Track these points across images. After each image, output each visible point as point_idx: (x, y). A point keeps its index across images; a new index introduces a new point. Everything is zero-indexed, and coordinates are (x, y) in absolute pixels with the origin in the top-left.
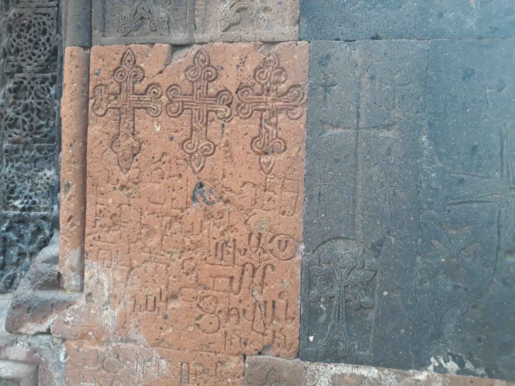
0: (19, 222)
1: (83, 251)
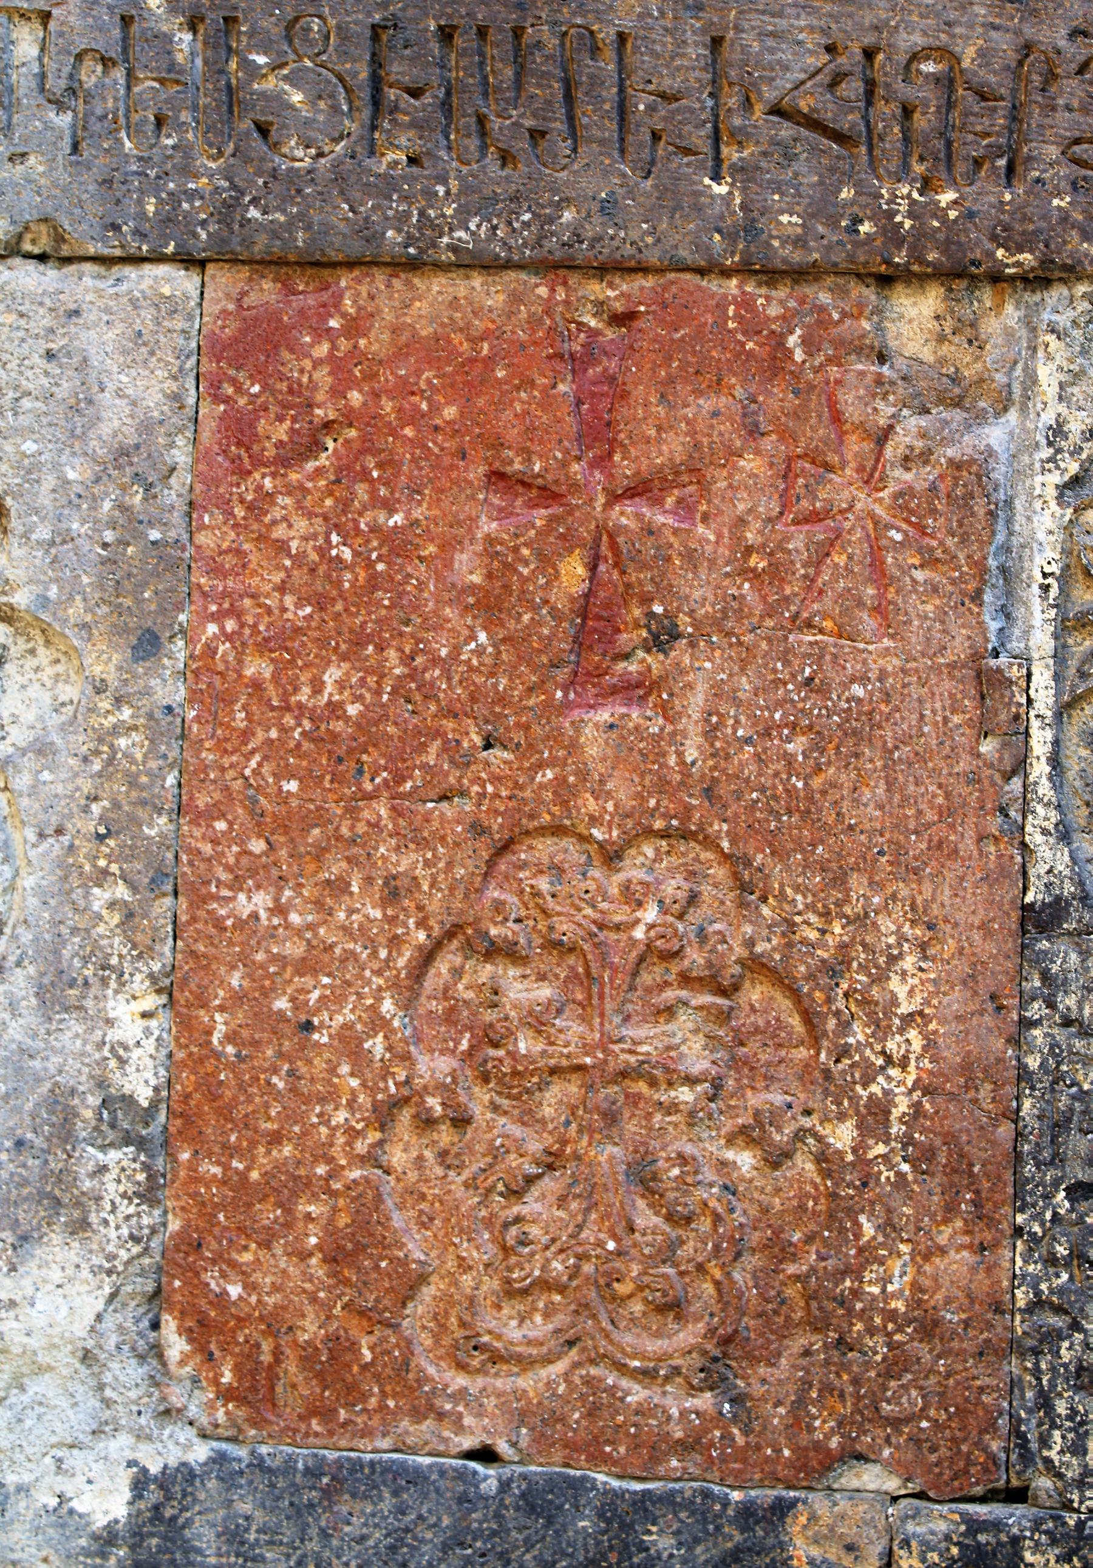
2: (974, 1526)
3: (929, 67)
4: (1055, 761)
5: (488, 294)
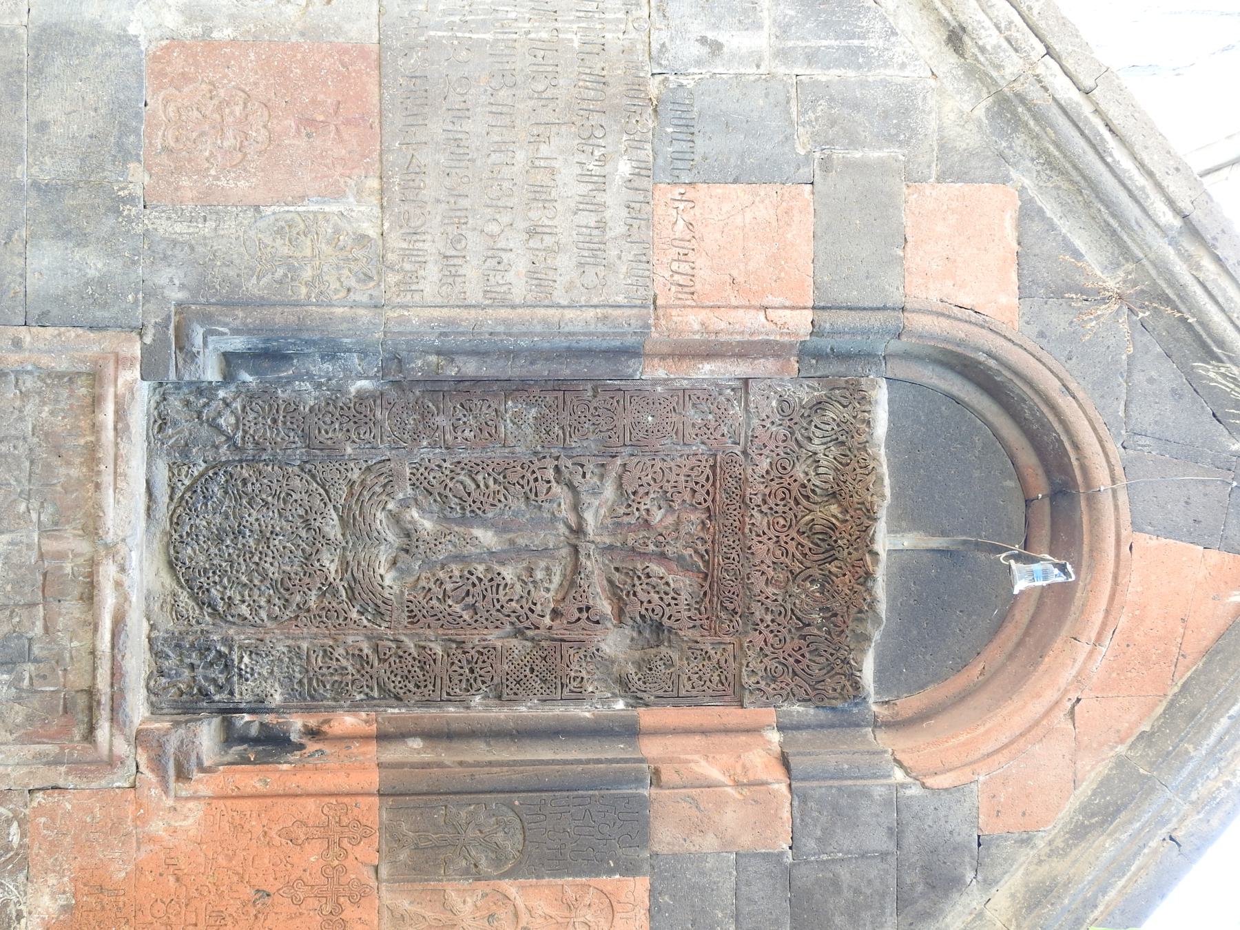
0: (226, 665)
5: (375, 100)
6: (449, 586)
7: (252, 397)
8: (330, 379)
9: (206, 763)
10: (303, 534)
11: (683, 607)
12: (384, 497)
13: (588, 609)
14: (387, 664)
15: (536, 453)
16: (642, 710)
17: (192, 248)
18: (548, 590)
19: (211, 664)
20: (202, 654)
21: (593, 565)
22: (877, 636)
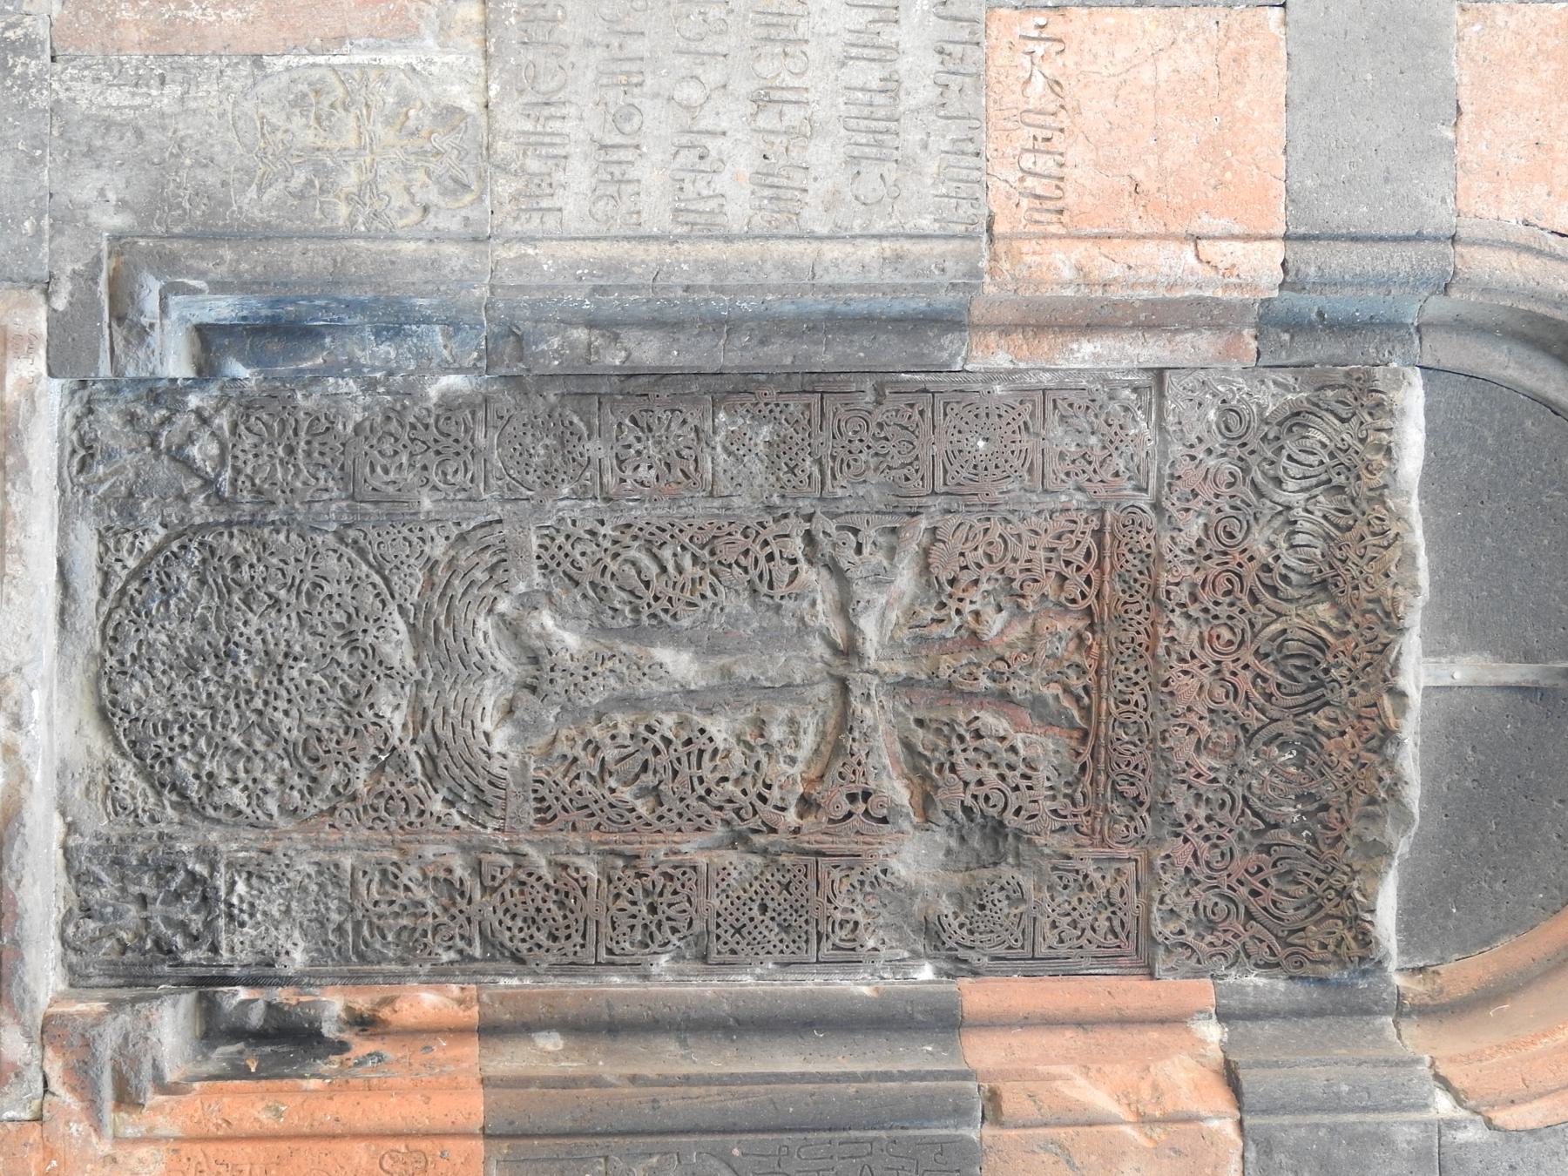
0: (205, 899)
1: (176, 1139)
2: (42, 43)
3: (560, 13)
4: (314, 65)
6: (610, 754)
7: (248, 406)
8: (391, 373)
9: (170, 1077)
10: (344, 657)
11: (1042, 792)
12: (491, 590)
13: (867, 795)
14: (497, 897)
15: (769, 508)
16: (965, 982)
17: (139, 134)
18: (792, 761)
19: (177, 896)
20: (160, 877)
21: (878, 718)
22: (1402, 847)
